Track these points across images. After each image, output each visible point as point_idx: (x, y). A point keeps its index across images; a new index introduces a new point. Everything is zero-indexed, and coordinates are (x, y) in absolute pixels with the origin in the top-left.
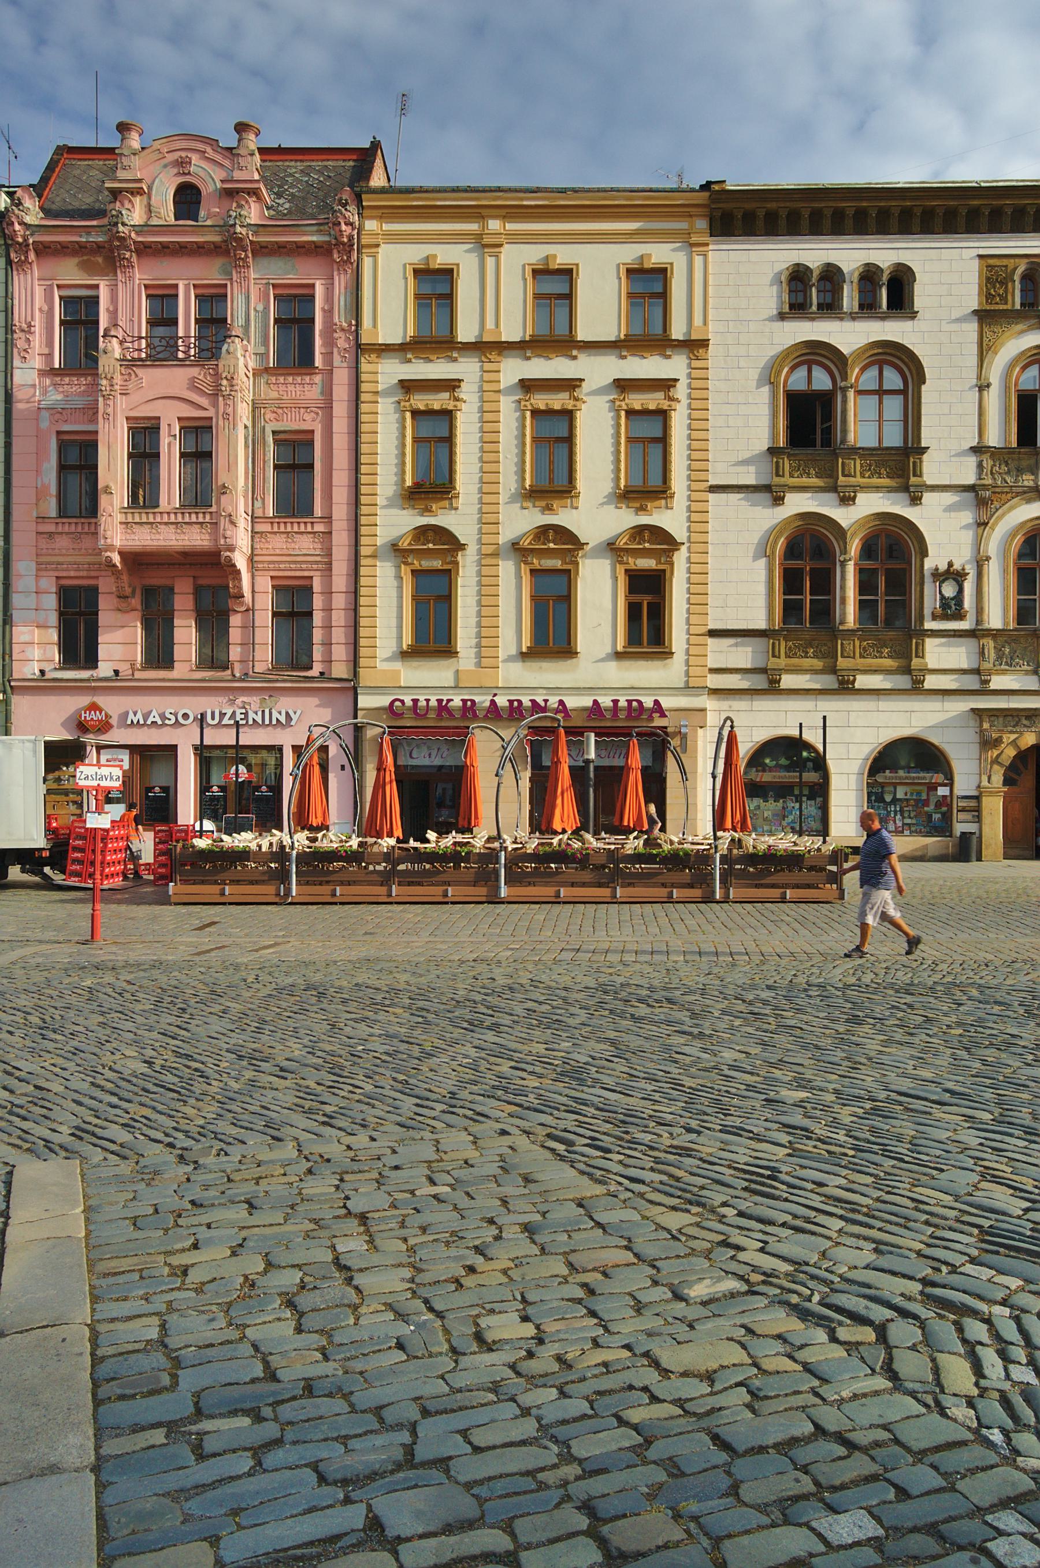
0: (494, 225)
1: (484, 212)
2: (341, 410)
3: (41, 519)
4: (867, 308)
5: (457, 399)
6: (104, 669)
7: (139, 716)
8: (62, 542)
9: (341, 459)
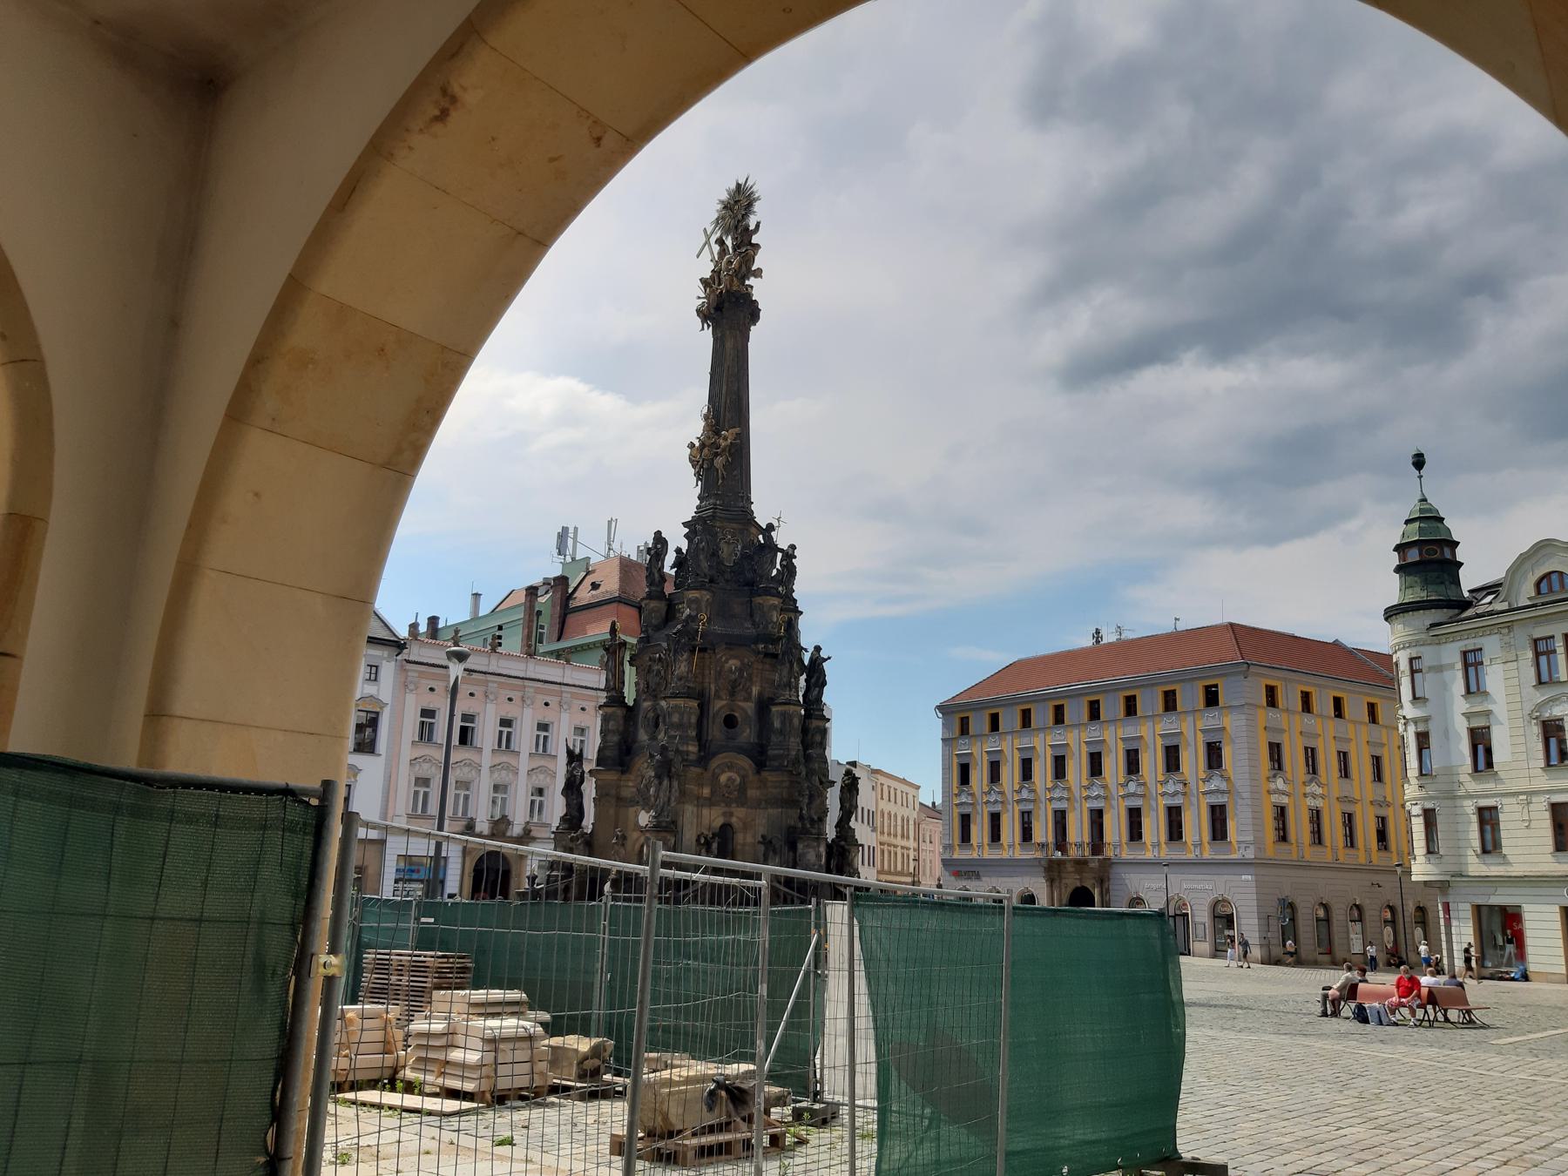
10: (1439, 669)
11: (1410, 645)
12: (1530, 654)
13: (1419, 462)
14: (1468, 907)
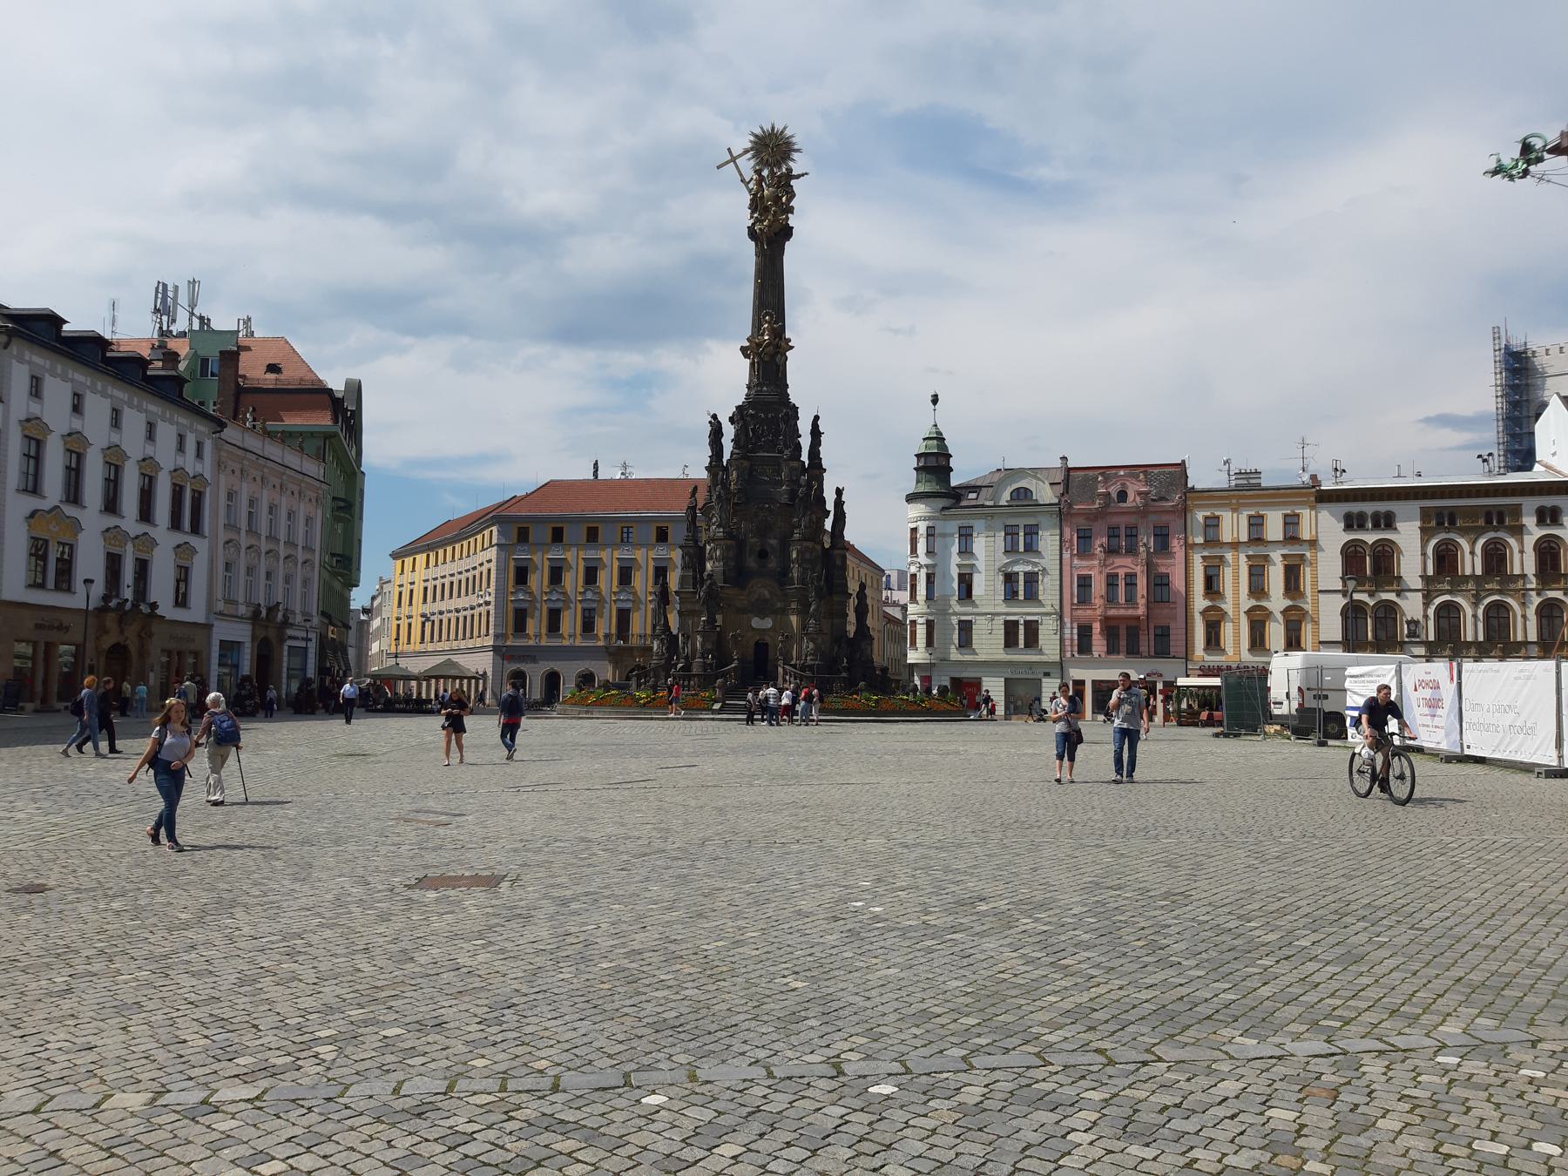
0: (1234, 501)
4: (1376, 526)
6: (1096, 654)
8: (1079, 612)
10: (944, 535)
11: (929, 519)
12: (1003, 534)
13: (935, 400)
14: (948, 678)
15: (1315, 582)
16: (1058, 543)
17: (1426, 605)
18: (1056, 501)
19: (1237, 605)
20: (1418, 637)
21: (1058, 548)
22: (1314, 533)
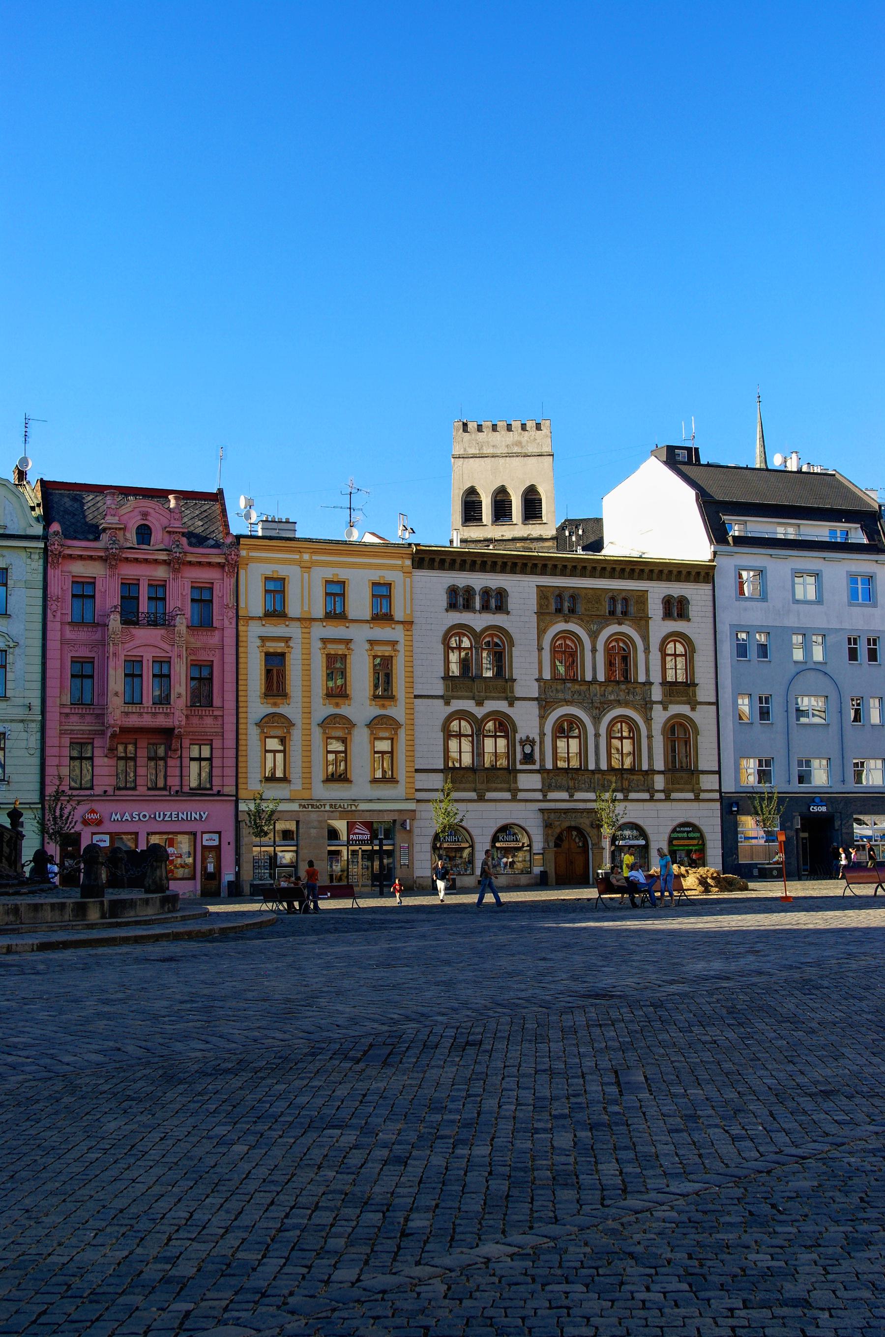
0: (306, 557)
1: (302, 550)
2: (230, 651)
3: (62, 706)
4: (485, 608)
5: (288, 647)
6: (98, 790)
7: (118, 815)
8: (74, 719)
9: (230, 677)
15: (411, 684)
16: (40, 602)
17: (543, 718)
18: (38, 530)
19: (308, 712)
20: (534, 764)
21: (39, 610)
22: (408, 612)
